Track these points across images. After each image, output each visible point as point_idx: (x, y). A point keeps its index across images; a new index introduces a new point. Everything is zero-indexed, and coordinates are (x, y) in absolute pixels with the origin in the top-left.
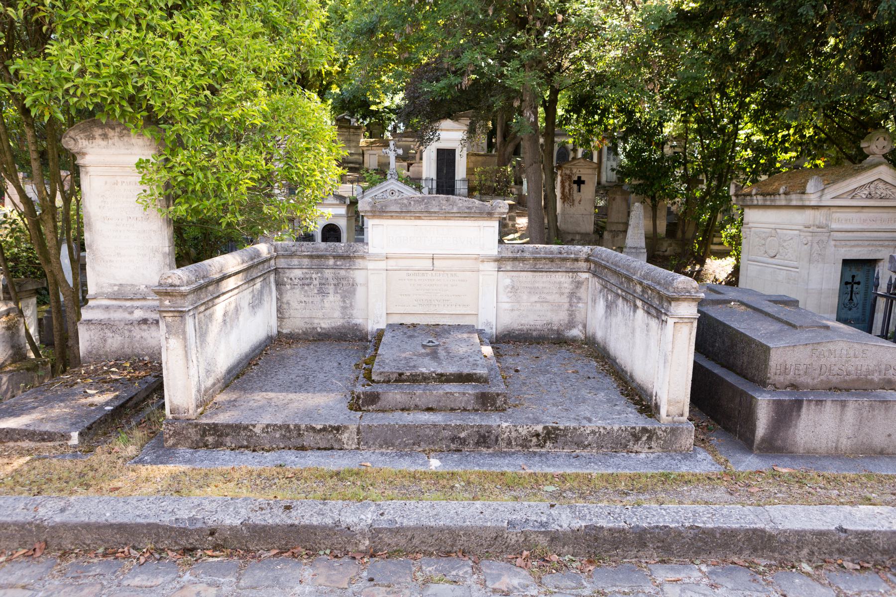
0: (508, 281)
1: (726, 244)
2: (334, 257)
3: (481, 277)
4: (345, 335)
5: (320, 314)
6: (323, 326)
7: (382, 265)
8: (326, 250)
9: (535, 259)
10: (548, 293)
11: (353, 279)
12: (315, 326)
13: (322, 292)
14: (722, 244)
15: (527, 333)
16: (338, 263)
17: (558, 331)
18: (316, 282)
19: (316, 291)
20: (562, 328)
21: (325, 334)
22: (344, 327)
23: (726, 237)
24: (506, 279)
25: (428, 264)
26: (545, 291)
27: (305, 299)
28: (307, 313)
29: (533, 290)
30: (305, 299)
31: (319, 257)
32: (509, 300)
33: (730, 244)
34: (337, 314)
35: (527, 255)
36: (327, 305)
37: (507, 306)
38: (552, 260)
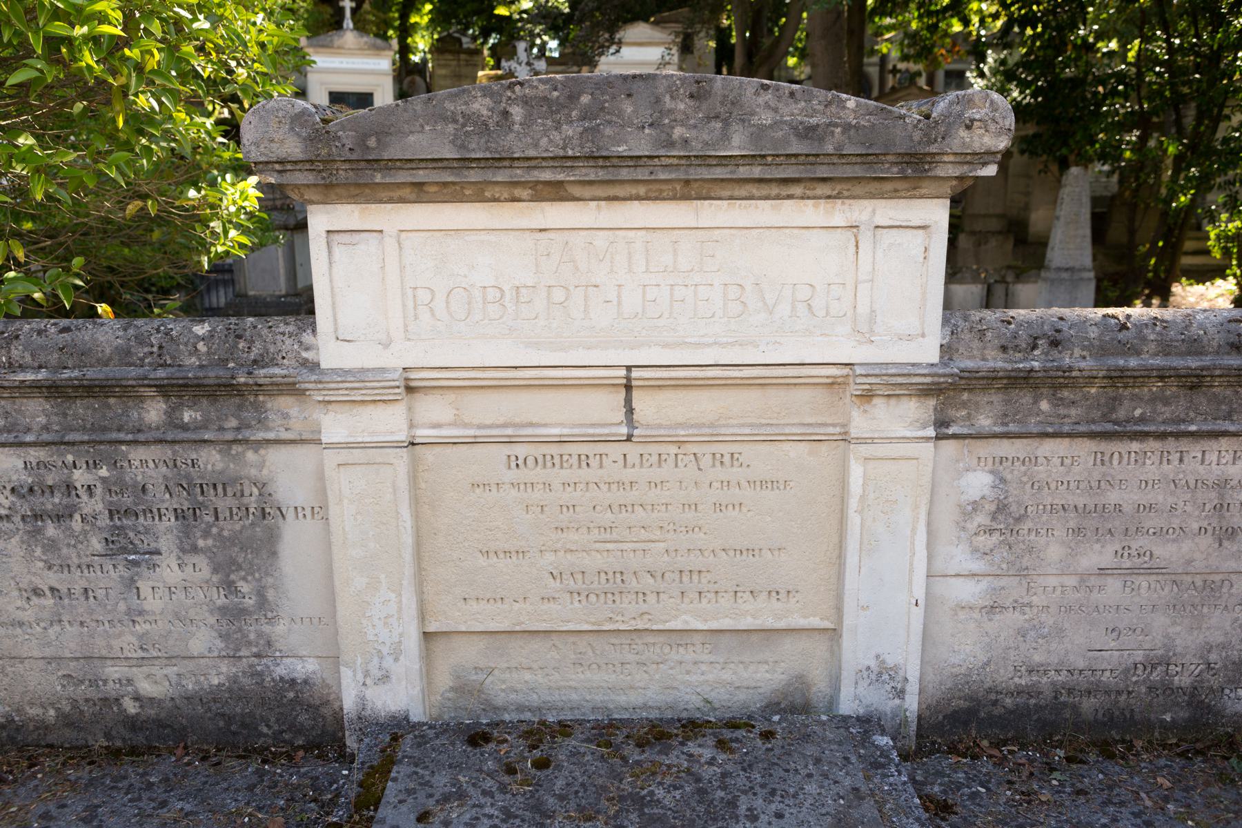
0: (978, 483)
1: (1217, 254)
2: (164, 390)
3: (856, 472)
4: (248, 724)
5: (127, 641)
6: (147, 688)
7: (389, 422)
8: (124, 355)
9: (1118, 378)
10: (1160, 533)
11: (262, 485)
12: (111, 689)
13: (125, 546)
14: (1207, 252)
15: (1057, 706)
16: (187, 416)
17: (1193, 692)
18: (94, 505)
19: (97, 545)
20: (1215, 682)
21: (160, 723)
22: (235, 691)
23: (1218, 237)
25: (605, 409)
27: (53, 578)
28: (69, 640)
29: (1092, 521)
30: (53, 578)
31: (90, 390)
32: (977, 566)
33: (1226, 252)
34: (203, 640)
35: (1075, 359)
36: (153, 603)
37: (968, 591)
38: (1194, 382)
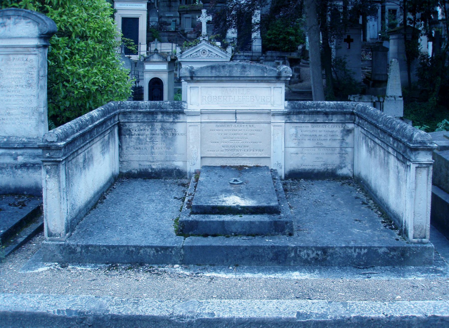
3: (272, 128)
7: (197, 119)
24: (292, 129)
26: (322, 138)
